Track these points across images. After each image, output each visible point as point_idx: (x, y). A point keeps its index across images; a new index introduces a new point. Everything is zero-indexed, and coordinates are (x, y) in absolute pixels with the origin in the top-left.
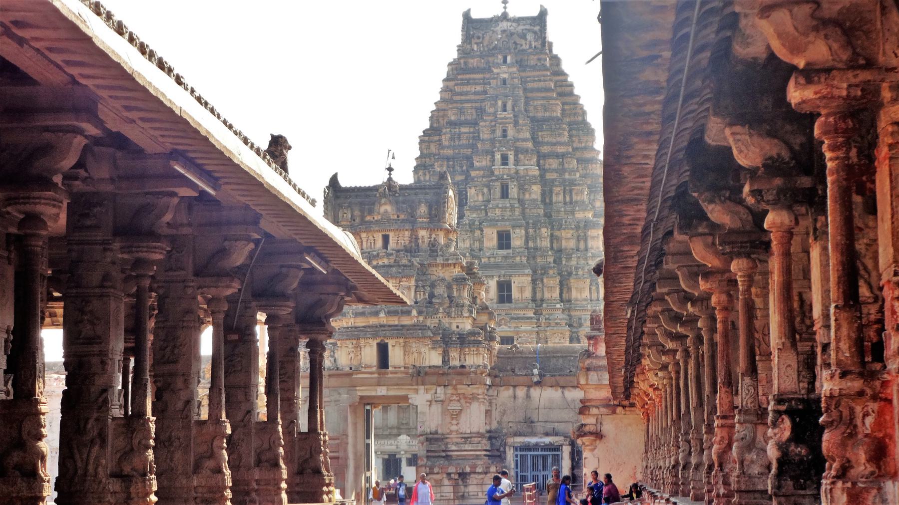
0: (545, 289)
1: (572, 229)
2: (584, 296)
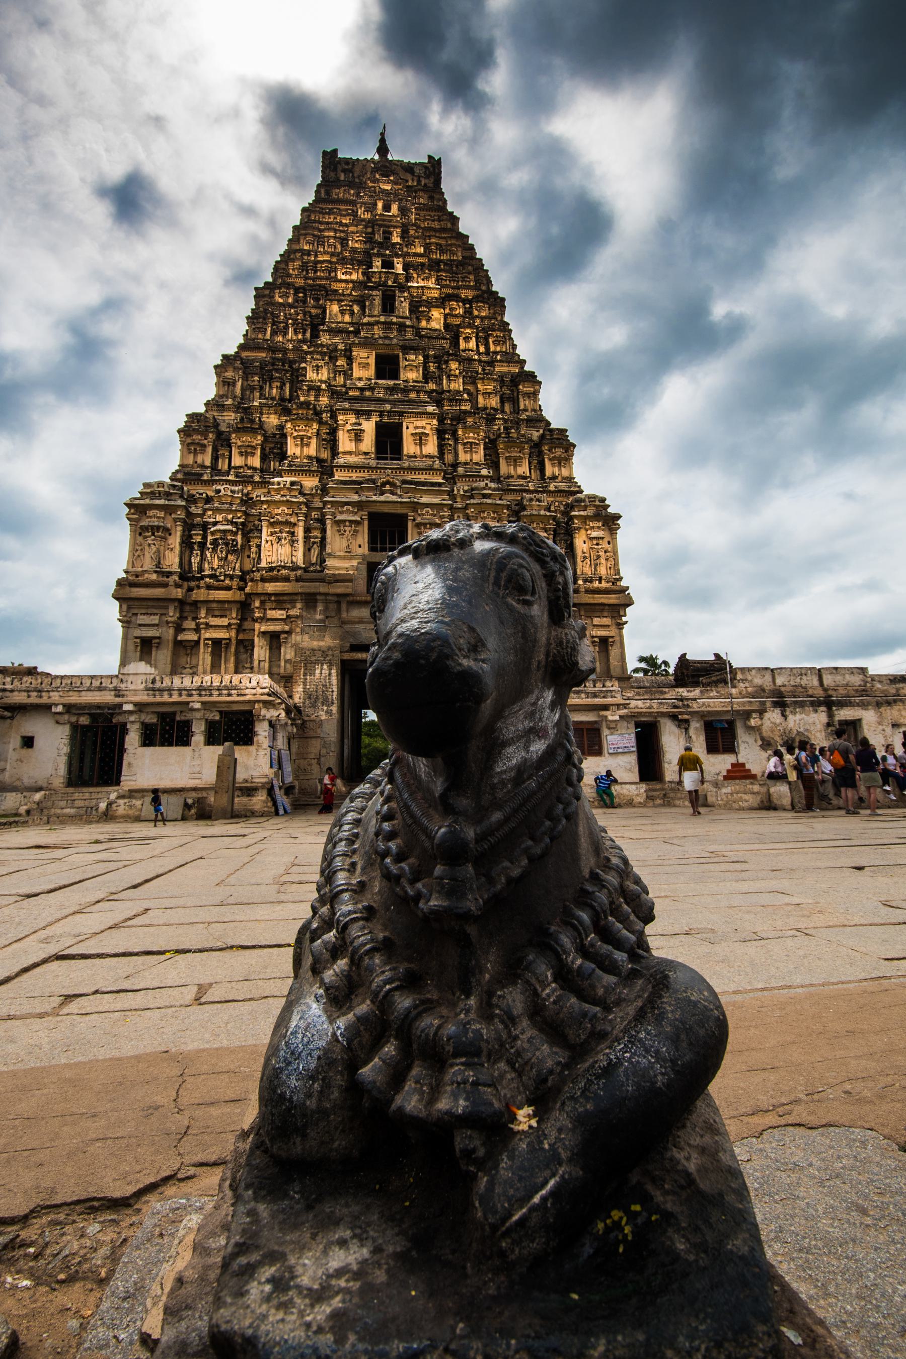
0: (460, 447)
1: (495, 380)
2: (520, 471)
